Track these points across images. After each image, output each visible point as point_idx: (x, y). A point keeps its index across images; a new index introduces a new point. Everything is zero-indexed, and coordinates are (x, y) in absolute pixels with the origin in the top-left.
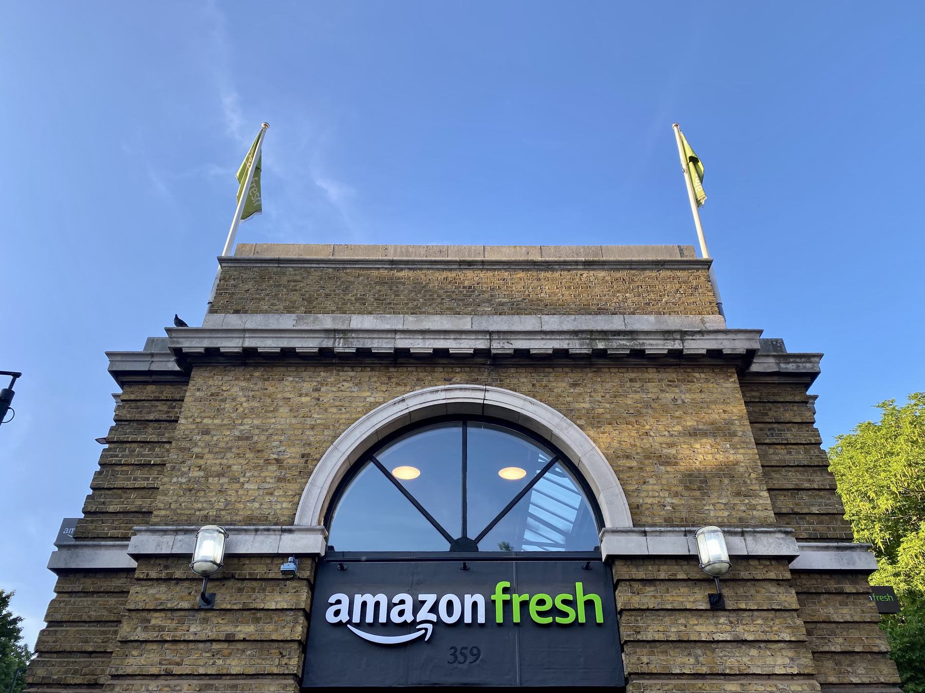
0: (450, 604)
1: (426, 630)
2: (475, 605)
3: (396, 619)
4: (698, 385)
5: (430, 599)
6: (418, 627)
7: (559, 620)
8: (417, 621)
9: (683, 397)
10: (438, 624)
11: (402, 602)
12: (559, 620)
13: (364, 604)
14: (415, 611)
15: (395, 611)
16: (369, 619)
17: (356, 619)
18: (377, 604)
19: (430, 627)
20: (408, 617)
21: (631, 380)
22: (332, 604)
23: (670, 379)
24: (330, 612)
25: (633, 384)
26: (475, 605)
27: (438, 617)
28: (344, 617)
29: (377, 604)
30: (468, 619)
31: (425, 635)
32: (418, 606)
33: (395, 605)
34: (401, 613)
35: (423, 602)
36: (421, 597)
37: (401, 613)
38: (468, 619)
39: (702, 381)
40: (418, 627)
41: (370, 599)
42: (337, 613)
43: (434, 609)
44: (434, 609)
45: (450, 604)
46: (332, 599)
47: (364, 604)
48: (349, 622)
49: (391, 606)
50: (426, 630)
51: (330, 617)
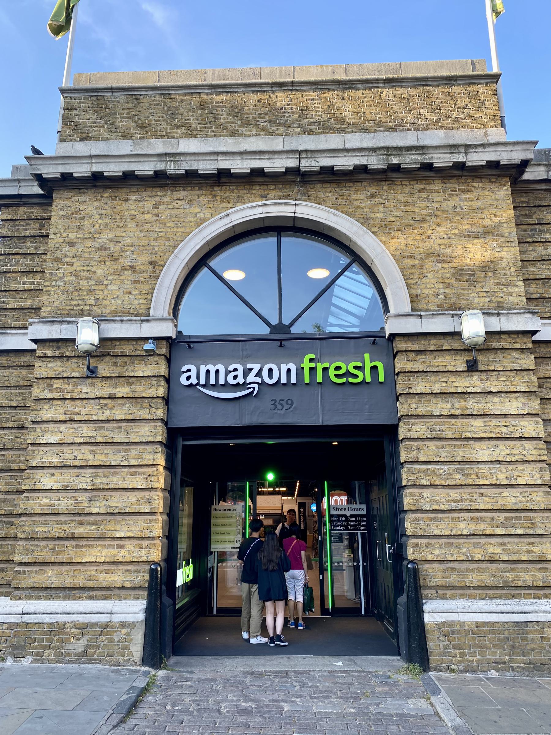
0: (270, 370)
1: (254, 388)
2: (289, 371)
3: (231, 381)
4: (475, 194)
5: (256, 367)
6: (248, 387)
7: (351, 380)
8: (247, 382)
9: (462, 204)
10: (262, 384)
11: (236, 370)
12: (351, 380)
13: (208, 372)
14: (245, 376)
16: (212, 381)
17: (203, 382)
18: (217, 371)
19: (256, 386)
20: (240, 380)
21: (420, 191)
23: (453, 189)
24: (184, 377)
25: (421, 195)
26: (289, 371)
27: (262, 380)
28: (194, 381)
29: (217, 371)
30: (284, 380)
31: (253, 392)
32: (247, 372)
33: (231, 372)
34: (235, 377)
35: (251, 370)
36: (249, 366)
37: (235, 377)
38: (284, 380)
39: (479, 190)
40: (248, 387)
41: (212, 369)
42: (188, 378)
45: (270, 370)
46: (184, 369)
47: (208, 372)
48: (198, 384)
49: (227, 373)
50: (254, 388)
51: (183, 381)
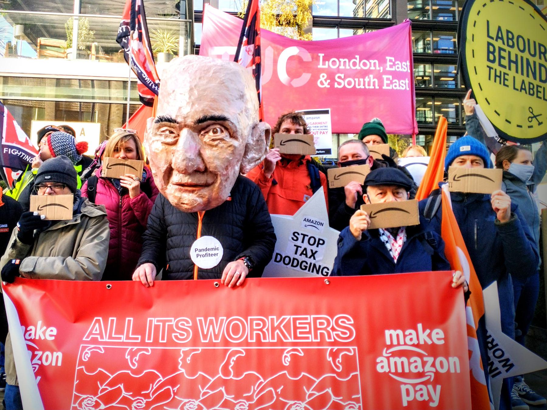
6: (426, 374)
10: (437, 373)
15: (413, 366)
16: (400, 370)
17: (393, 370)
19: (433, 375)
20: (420, 369)
22: (378, 363)
28: (387, 370)
40: (426, 374)
42: (382, 367)
43: (433, 365)
44: (433, 365)
45: (441, 363)
48: (390, 372)
49: (410, 364)
50: (430, 376)
